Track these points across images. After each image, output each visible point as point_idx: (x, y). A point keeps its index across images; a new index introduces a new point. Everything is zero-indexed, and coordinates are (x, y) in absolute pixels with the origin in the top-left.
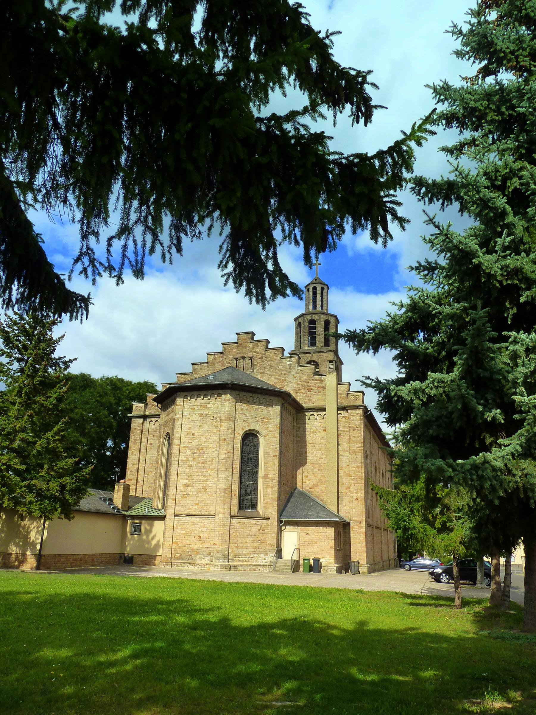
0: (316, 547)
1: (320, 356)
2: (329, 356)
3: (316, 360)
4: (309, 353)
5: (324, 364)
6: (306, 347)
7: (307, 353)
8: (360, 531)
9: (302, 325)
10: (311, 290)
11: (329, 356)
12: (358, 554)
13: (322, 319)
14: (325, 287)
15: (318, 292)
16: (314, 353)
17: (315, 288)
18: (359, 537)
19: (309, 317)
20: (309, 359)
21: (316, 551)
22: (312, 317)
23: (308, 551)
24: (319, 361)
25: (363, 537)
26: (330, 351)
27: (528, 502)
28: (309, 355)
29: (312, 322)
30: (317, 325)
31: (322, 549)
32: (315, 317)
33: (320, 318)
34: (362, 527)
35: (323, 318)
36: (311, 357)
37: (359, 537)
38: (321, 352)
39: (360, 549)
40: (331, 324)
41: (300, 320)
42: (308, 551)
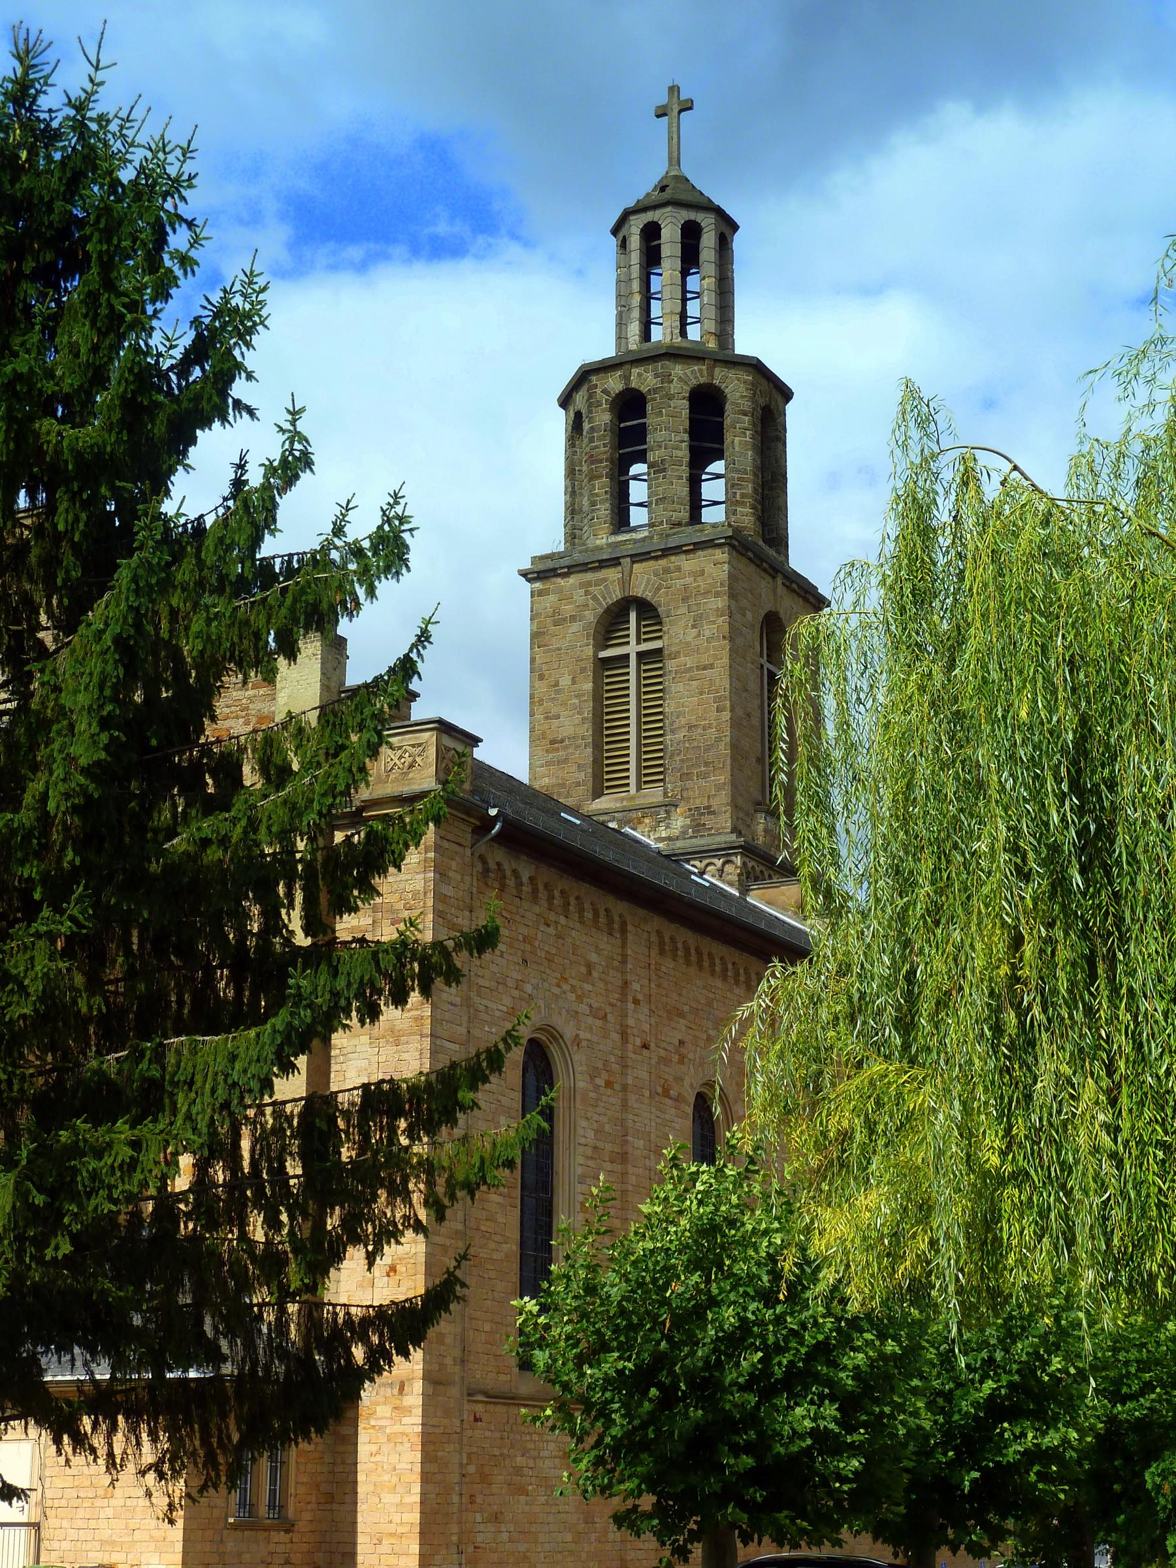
0: (109, 1512)
1: (666, 571)
2: (709, 569)
3: (648, 595)
4: (614, 562)
5: (683, 610)
6: (602, 539)
7: (603, 564)
8: (398, 1428)
9: (586, 426)
10: (635, 241)
11: (709, 569)
12: (385, 1548)
13: (675, 387)
14: (707, 221)
15: (666, 251)
16: (638, 558)
17: (651, 232)
18: (394, 1459)
19: (614, 383)
20: (617, 595)
21: (105, 1534)
22: (627, 378)
23: (73, 1534)
24: (661, 600)
25: (410, 1459)
26: (709, 544)
27: (389, 1194)
28: (612, 574)
29: (631, 405)
30: (651, 420)
31: (133, 1524)
32: (644, 379)
33: (667, 378)
34: (407, 1411)
35: (684, 377)
36: (624, 583)
37: (394, 1459)
38: (666, 552)
39: (396, 1518)
40: (728, 407)
41: (580, 399)
42: (73, 1534)
